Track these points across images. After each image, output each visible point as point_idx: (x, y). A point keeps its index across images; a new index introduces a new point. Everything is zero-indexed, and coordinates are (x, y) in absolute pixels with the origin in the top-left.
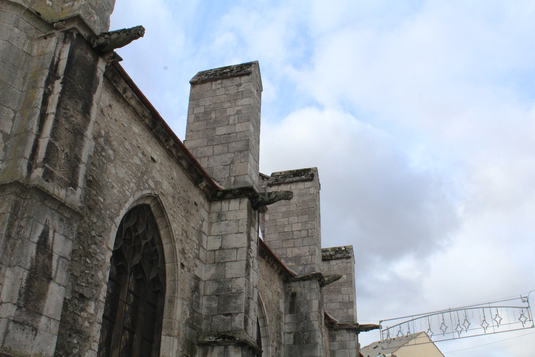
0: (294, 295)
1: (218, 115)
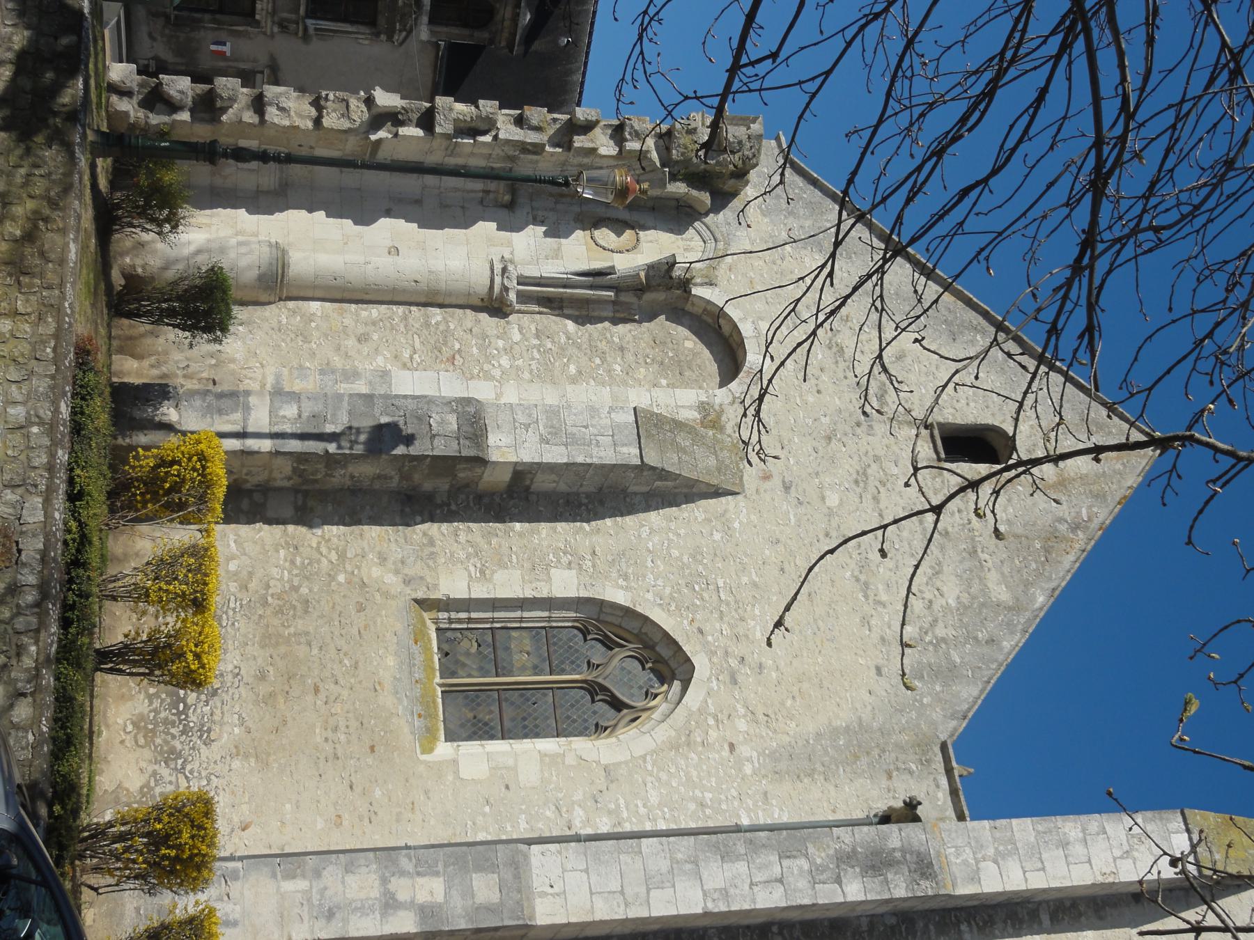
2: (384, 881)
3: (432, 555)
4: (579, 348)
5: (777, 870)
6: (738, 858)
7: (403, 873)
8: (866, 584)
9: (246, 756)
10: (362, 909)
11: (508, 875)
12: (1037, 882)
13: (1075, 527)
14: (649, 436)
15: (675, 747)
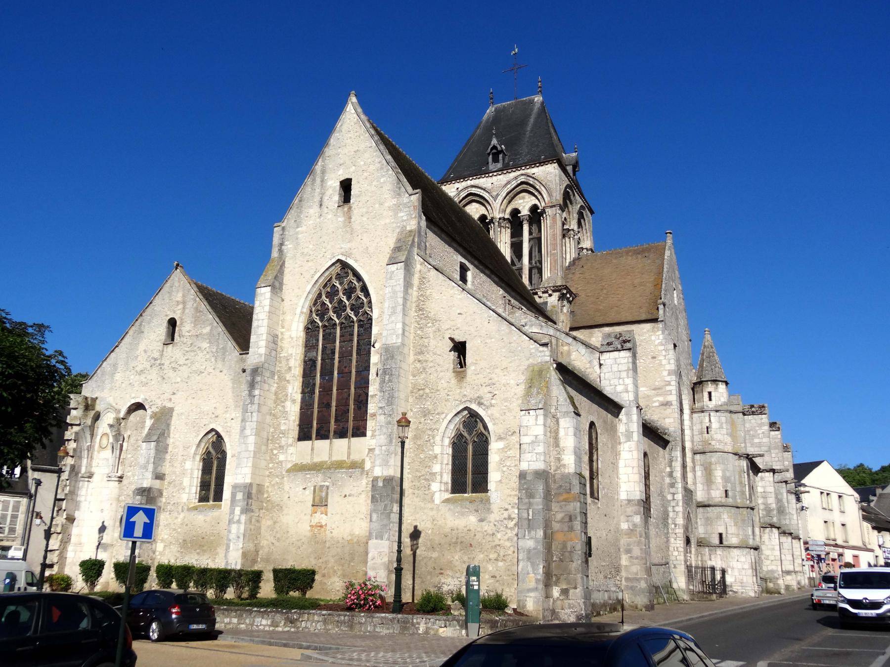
2: (234, 523)
3: (177, 504)
4: (135, 454)
5: (250, 414)
6: (245, 425)
7: (233, 518)
8: (201, 372)
9: (215, 558)
10: (239, 529)
11: (238, 489)
12: (264, 337)
14: (149, 439)
15: (230, 436)
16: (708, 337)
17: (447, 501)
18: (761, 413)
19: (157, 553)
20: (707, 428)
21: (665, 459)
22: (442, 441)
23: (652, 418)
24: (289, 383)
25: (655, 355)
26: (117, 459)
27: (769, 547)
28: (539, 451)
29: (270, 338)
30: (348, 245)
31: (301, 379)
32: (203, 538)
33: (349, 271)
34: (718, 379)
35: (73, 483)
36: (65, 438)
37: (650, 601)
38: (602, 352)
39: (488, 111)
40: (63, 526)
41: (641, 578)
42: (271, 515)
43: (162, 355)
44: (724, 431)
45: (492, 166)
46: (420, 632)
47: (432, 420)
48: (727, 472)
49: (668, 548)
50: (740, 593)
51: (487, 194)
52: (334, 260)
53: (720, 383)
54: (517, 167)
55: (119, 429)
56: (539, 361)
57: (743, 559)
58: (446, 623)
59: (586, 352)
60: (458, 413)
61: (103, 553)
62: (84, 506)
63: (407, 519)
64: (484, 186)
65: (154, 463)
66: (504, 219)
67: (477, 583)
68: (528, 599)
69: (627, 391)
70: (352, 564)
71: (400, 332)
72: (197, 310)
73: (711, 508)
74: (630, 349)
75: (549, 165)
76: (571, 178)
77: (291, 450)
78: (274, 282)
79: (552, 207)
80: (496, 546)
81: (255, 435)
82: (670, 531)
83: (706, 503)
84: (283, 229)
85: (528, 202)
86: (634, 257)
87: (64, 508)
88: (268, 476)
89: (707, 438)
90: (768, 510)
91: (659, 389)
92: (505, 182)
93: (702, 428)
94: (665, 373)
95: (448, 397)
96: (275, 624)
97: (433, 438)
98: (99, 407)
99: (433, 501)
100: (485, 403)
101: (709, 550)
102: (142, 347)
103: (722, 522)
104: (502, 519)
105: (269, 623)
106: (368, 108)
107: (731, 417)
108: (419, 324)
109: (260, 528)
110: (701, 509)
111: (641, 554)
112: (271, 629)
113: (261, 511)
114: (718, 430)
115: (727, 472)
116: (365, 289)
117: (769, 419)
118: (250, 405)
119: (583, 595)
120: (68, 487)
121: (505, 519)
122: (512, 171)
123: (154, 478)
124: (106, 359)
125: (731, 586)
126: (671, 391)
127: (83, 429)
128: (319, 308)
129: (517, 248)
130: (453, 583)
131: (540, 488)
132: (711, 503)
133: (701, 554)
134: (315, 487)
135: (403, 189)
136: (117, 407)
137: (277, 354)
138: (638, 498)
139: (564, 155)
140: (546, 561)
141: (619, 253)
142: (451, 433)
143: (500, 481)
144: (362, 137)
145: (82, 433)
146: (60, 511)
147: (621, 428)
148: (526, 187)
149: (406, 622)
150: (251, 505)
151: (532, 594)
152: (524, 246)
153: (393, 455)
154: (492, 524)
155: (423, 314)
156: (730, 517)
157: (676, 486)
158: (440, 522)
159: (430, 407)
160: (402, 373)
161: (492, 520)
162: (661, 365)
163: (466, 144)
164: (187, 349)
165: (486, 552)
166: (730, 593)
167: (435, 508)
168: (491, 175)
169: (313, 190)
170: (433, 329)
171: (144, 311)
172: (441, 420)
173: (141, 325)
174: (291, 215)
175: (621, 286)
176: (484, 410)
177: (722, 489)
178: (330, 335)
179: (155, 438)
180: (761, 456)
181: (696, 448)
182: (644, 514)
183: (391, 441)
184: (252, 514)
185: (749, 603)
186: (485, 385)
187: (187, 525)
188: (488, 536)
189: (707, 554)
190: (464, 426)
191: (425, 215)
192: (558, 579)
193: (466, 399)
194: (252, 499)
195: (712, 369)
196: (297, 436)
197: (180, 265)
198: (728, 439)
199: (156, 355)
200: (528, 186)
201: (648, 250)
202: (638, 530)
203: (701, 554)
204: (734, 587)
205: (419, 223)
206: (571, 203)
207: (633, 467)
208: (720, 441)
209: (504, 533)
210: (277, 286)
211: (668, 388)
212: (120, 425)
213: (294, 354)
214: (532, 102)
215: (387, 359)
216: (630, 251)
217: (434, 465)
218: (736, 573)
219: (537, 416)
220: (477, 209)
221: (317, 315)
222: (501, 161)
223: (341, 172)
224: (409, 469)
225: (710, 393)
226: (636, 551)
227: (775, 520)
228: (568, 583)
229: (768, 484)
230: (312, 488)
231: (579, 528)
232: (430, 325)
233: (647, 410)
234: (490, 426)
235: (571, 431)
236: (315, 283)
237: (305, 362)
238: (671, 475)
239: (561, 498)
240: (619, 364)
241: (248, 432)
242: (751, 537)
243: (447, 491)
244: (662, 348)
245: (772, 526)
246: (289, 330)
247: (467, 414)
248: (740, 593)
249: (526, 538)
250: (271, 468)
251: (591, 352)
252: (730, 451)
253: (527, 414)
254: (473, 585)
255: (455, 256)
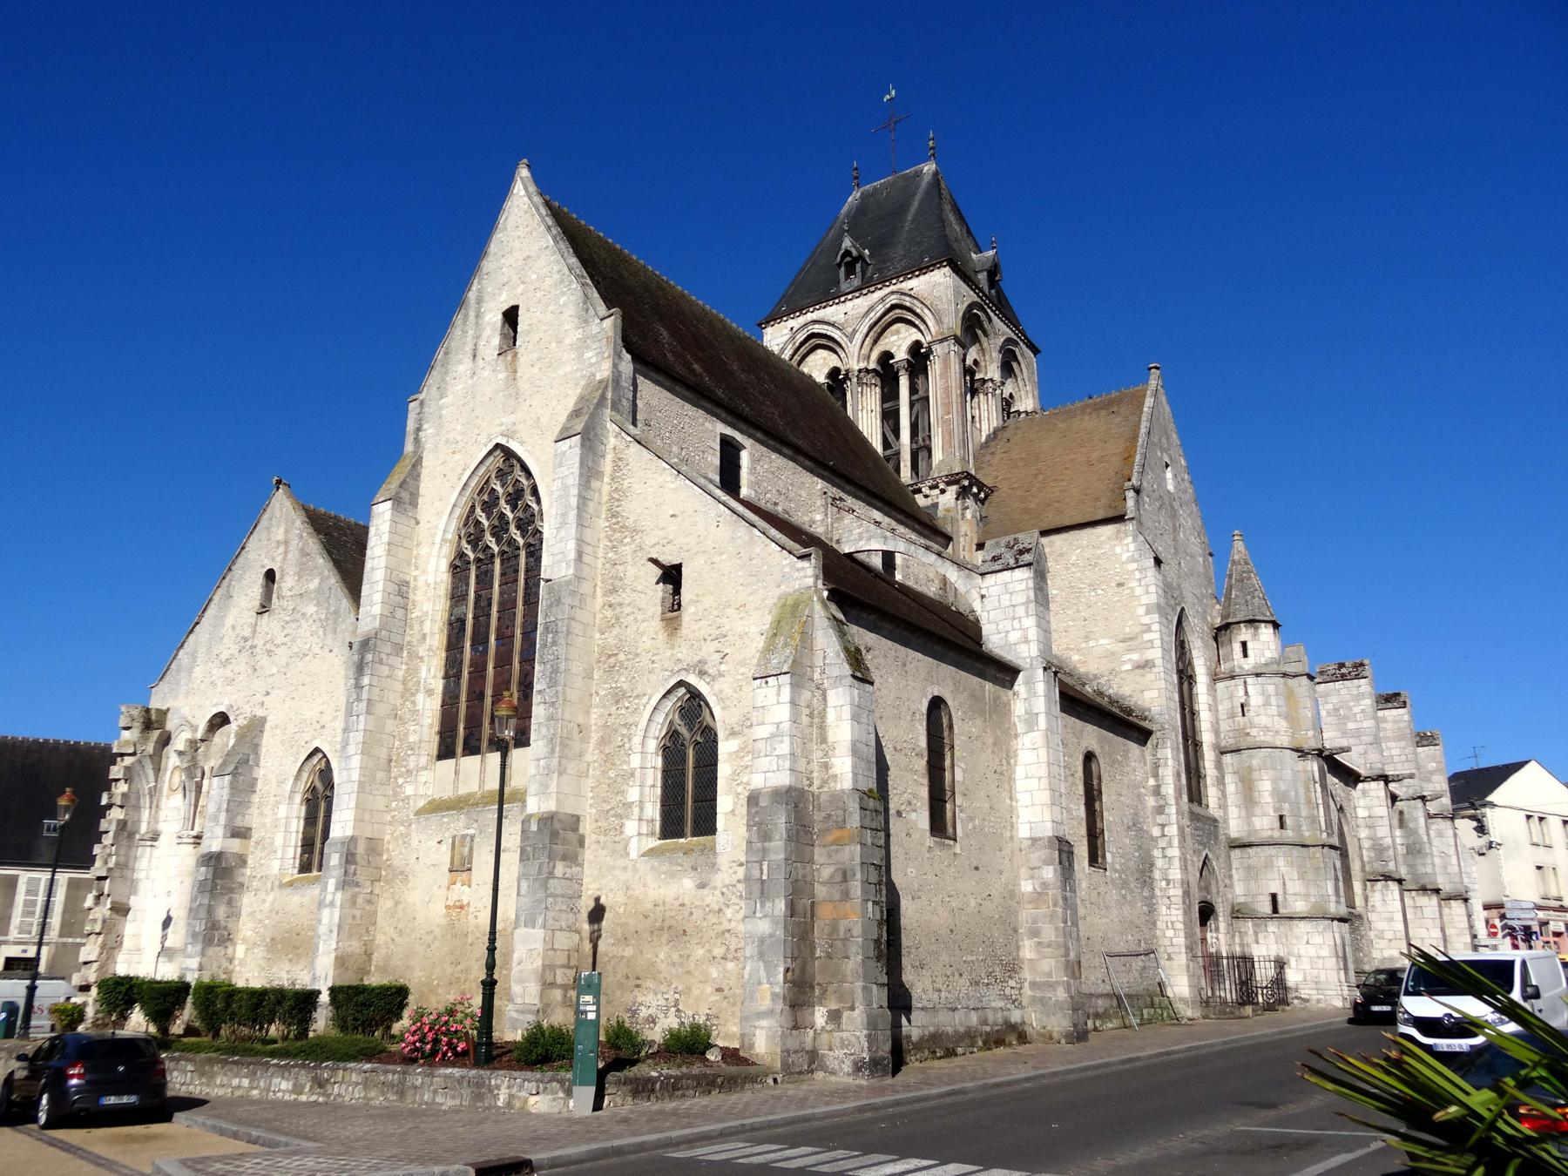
0: (1401, 813)
1: (1346, 712)
2: (326, 906)
12: (380, 586)
13: (301, 537)
14: (223, 770)
16: (1239, 546)
17: (651, 853)
18: (1357, 677)
19: (236, 962)
20: (1242, 706)
21: (1145, 764)
22: (643, 744)
23: (1120, 693)
24: (422, 662)
25: (1122, 581)
26: (192, 807)
27: (1383, 915)
28: (781, 753)
29: (392, 588)
30: (512, 418)
31: (444, 654)
32: (298, 934)
33: (515, 462)
34: (1257, 618)
35: (123, 852)
36: (111, 777)
37: (1075, 1025)
38: (982, 575)
39: (850, 199)
40: (104, 921)
41: (1057, 982)
42: (392, 890)
43: (254, 632)
44: (1274, 710)
45: (844, 286)
46: (500, 1103)
47: (627, 708)
48: (1280, 783)
49: (1154, 924)
50: (1314, 1002)
51: (838, 332)
52: (490, 447)
53: (1263, 625)
54: (884, 281)
55: (194, 758)
56: (797, 587)
57: (1318, 939)
58: (538, 1087)
59: (959, 576)
60: (669, 692)
61: (168, 964)
62: (144, 886)
63: (588, 889)
64: (832, 320)
65: (228, 811)
66: (867, 371)
67: (594, 1008)
68: (758, 1032)
69: (1026, 641)
70: (505, 972)
71: (572, 555)
72: (304, 553)
73: (1254, 849)
74: (1029, 565)
75: (936, 272)
76: (984, 294)
77: (424, 776)
78: (397, 493)
79: (941, 341)
80: (723, 933)
81: (362, 753)
82: (1158, 892)
83: (1246, 841)
84: (422, 403)
85: (905, 338)
86: (1094, 415)
87: (106, 892)
88: (390, 823)
89: (1242, 724)
90: (1379, 849)
91: (1131, 639)
92: (866, 309)
93: (1232, 707)
94: (1141, 611)
95: (654, 665)
96: (298, 1089)
97: (630, 740)
98: (170, 725)
99: (628, 854)
100: (710, 671)
101: (1254, 925)
102: (229, 620)
103: (1276, 872)
104: (735, 882)
105: (290, 1087)
106: (542, 182)
107: (1285, 684)
108: (611, 541)
109: (375, 913)
110: (1236, 853)
111: (1057, 937)
112: (293, 1097)
113: (377, 884)
114: (1262, 709)
115: (1280, 783)
116: (535, 492)
117: (1374, 685)
118: (356, 703)
119: (865, 1020)
120: (114, 857)
121: (739, 881)
122: (876, 289)
123: (229, 835)
124: (182, 646)
125: (1297, 990)
126: (1151, 641)
127: (140, 762)
128: (472, 530)
129: (890, 417)
130: (654, 1003)
131: (780, 822)
132: (1253, 839)
133: (1240, 932)
134: (454, 837)
135: (592, 312)
136: (194, 722)
137: (406, 615)
138: (1050, 834)
139: (974, 255)
140: (794, 959)
141: (1070, 411)
142: (661, 730)
143: (733, 811)
144: (534, 233)
145: (138, 768)
146: (102, 898)
147: (1018, 708)
148: (900, 314)
149: (479, 1084)
150: (355, 874)
151: (764, 1023)
152: (901, 413)
153: (556, 774)
154: (717, 892)
155: (618, 523)
156: (1291, 864)
157: (1167, 811)
158: (637, 892)
159: (625, 686)
160: (577, 628)
161: (719, 884)
162: (1133, 596)
163: (812, 255)
164: (287, 618)
165: (707, 945)
166: (1296, 1001)
167: (630, 865)
168: (842, 299)
169: (465, 332)
170: (633, 546)
171: (234, 563)
172: (642, 708)
173: (228, 587)
174: (433, 379)
175: (1068, 466)
176: (708, 683)
177: (1272, 814)
178: (486, 575)
179: (230, 769)
180: (1347, 750)
181: (1223, 743)
182: (1060, 863)
183: (553, 750)
184: (357, 889)
185: (1306, 1021)
186: (711, 638)
187: (277, 913)
188: (711, 915)
189: (1251, 932)
190: (682, 717)
191: (629, 351)
192: (824, 992)
193: (680, 666)
194: (355, 863)
195: (1247, 601)
196: (435, 752)
197: (284, 481)
198: (1282, 725)
199: (247, 632)
200: (904, 312)
201: (1119, 401)
202: (1050, 892)
203: (1240, 932)
204: (1302, 991)
205: (615, 366)
206: (986, 335)
207: (1040, 778)
208: (1267, 729)
209: (737, 907)
210: (406, 501)
211: (1147, 637)
212: (196, 750)
213: (430, 612)
214: (919, 174)
215: (551, 605)
216: (1088, 406)
217: (630, 789)
218: (1306, 965)
219: (780, 686)
220: (825, 359)
221: (469, 543)
222: (859, 274)
223: (503, 297)
224: (592, 798)
225: (1244, 644)
226: (1049, 933)
227: (1391, 866)
228: (841, 999)
229: (1376, 802)
230: (450, 841)
231: (859, 893)
232: (628, 540)
233: (1111, 677)
234: (717, 711)
235: (847, 713)
236: (463, 489)
237: (450, 624)
238: (1157, 791)
239: (830, 838)
240: (1011, 594)
241: (352, 749)
242: (1333, 899)
243: (653, 834)
244: (1134, 566)
245: (1387, 878)
246: (424, 572)
247: (685, 694)
248: (1314, 1002)
249: (758, 915)
250: (395, 810)
251: (968, 576)
252: (1286, 744)
253: (764, 685)
254: (586, 1012)
255: (707, 424)
